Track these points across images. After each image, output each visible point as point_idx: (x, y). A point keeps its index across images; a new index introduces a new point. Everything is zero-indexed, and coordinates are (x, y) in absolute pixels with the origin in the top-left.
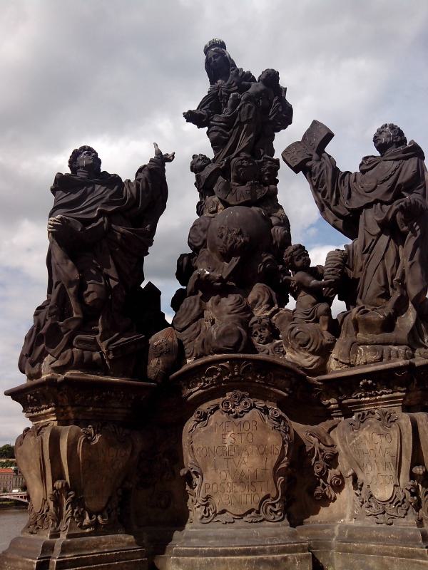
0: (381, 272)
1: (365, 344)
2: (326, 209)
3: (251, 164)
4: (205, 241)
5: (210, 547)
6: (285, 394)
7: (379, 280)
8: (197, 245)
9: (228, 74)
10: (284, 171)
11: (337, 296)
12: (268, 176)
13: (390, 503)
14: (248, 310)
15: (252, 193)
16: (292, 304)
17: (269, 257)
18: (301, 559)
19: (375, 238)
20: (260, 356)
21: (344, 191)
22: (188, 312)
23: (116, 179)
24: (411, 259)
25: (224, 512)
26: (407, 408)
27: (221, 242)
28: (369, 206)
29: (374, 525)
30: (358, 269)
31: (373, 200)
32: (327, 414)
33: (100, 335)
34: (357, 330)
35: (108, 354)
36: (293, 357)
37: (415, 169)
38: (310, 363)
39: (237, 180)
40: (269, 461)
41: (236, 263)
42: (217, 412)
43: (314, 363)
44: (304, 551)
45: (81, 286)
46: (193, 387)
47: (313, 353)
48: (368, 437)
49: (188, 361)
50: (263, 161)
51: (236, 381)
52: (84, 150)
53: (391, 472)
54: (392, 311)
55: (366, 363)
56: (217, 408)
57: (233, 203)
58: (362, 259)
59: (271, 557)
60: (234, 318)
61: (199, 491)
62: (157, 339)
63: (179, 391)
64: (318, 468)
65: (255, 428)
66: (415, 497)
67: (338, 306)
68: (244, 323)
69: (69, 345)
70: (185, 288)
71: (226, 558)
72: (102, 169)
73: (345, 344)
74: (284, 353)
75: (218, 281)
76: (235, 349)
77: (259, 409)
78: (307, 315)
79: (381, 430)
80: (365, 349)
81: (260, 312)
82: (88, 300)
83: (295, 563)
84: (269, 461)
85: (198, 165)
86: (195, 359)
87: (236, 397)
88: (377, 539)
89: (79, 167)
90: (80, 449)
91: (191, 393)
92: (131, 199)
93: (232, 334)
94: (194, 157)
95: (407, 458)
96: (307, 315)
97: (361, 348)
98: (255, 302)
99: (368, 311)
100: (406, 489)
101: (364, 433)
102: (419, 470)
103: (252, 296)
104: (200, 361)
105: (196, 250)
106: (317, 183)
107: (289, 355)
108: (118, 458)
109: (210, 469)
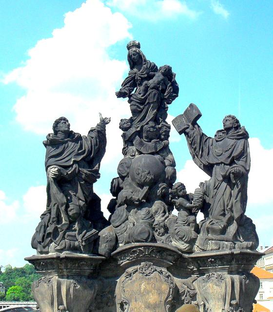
0: (222, 202)
2: (196, 157)
3: (155, 130)
4: (128, 173)
7: (220, 206)
8: (124, 175)
9: (141, 64)
10: (173, 132)
12: (164, 135)
14: (152, 217)
15: (156, 148)
16: (175, 212)
17: (164, 186)
19: (220, 182)
21: (206, 150)
22: (120, 217)
24: (236, 199)
26: (230, 273)
27: (138, 177)
28: (218, 164)
30: (211, 197)
31: (220, 162)
32: (193, 273)
33: (77, 232)
34: (208, 232)
35: (82, 242)
36: (176, 244)
37: (242, 147)
39: (147, 137)
41: (146, 190)
42: (137, 273)
45: (67, 207)
47: (186, 242)
49: (120, 245)
52: (61, 120)
53: (221, 303)
54: (226, 224)
55: (212, 250)
56: (137, 271)
58: (214, 192)
60: (145, 222)
62: (104, 233)
63: (117, 260)
67: (200, 216)
68: (151, 225)
69: (64, 238)
70: (115, 198)
73: (202, 239)
75: (137, 201)
76: (146, 241)
78: (184, 221)
80: (212, 242)
81: (158, 218)
82: (71, 213)
85: (125, 126)
86: (125, 244)
87: (147, 265)
89: (59, 131)
90: (71, 290)
91: (122, 263)
92: (89, 150)
93: (145, 232)
94: (121, 120)
95: (229, 296)
96: (184, 221)
98: (156, 212)
101: (209, 284)
102: (234, 302)
104: (128, 246)
105: (123, 178)
106: (192, 142)
107: (173, 243)
108: (88, 295)
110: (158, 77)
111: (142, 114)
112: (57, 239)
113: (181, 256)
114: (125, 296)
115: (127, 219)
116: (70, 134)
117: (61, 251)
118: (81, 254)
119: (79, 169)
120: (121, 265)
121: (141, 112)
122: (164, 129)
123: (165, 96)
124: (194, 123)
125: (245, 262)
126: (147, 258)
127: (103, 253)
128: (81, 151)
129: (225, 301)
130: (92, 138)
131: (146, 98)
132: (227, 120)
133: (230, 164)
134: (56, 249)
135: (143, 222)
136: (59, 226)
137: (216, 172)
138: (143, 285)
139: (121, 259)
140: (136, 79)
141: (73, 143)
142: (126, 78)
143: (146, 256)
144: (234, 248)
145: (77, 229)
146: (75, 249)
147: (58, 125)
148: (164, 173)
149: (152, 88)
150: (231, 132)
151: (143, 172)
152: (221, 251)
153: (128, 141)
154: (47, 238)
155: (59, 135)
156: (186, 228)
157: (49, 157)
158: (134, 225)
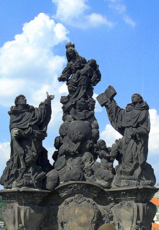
3: (85, 104)
4: (66, 134)
6: (96, 196)
7: (130, 156)
8: (63, 135)
9: (75, 59)
10: (97, 105)
12: (91, 107)
14: (83, 163)
15: (85, 116)
16: (99, 160)
20: (87, 182)
21: (120, 118)
22: (61, 164)
24: (140, 151)
26: (136, 202)
27: (73, 136)
28: (128, 127)
30: (123, 150)
33: (31, 174)
34: (121, 174)
35: (35, 181)
36: (99, 182)
38: (105, 184)
39: (79, 109)
41: (79, 145)
42: (72, 202)
43: (107, 184)
45: (25, 156)
46: (63, 192)
47: (106, 181)
49: (61, 183)
50: (89, 101)
53: (130, 222)
54: (133, 168)
55: (124, 186)
56: (72, 200)
58: (125, 146)
60: (78, 167)
61: (66, 229)
62: (50, 174)
63: (58, 193)
64: (106, 221)
67: (116, 163)
69: (22, 178)
70: (57, 150)
73: (117, 179)
74: (96, 180)
75: (72, 153)
76: (79, 180)
79: (128, 209)
80: (124, 181)
81: (87, 164)
82: (27, 161)
85: (64, 101)
87: (79, 196)
90: (27, 214)
91: (62, 195)
92: (39, 117)
93: (78, 174)
95: (135, 218)
97: (122, 180)
98: (86, 160)
99: (125, 168)
101: (122, 210)
102: (139, 222)
103: (84, 157)
104: (66, 183)
105: (62, 136)
106: (110, 112)
107: (97, 181)
108: (39, 217)
109: (70, 221)
110: (87, 67)
111: (76, 93)
112: (18, 179)
113: (102, 190)
114: (64, 218)
115: (66, 165)
116: (27, 107)
117: (20, 187)
118: (34, 189)
119: (33, 131)
120: (62, 196)
121: (75, 91)
122: (91, 103)
123: (92, 80)
124: (112, 99)
126: (80, 192)
127: (49, 188)
128: (34, 118)
129: (133, 221)
130: (42, 109)
131: (78, 82)
132: (134, 97)
133: (136, 127)
134: (17, 185)
135: (77, 167)
136: (19, 170)
137: (126, 132)
138: (76, 210)
139: (62, 193)
140: (72, 68)
141: (29, 113)
142: (65, 68)
143: (78, 190)
144: (139, 185)
145: (32, 172)
146: (30, 186)
147: (18, 100)
148: (91, 133)
149: (83, 75)
150: (137, 105)
151: (77, 132)
152: (130, 187)
153: (66, 111)
154: (11, 177)
155: (19, 107)
156: (106, 170)
157: (12, 122)
158: (70, 169)
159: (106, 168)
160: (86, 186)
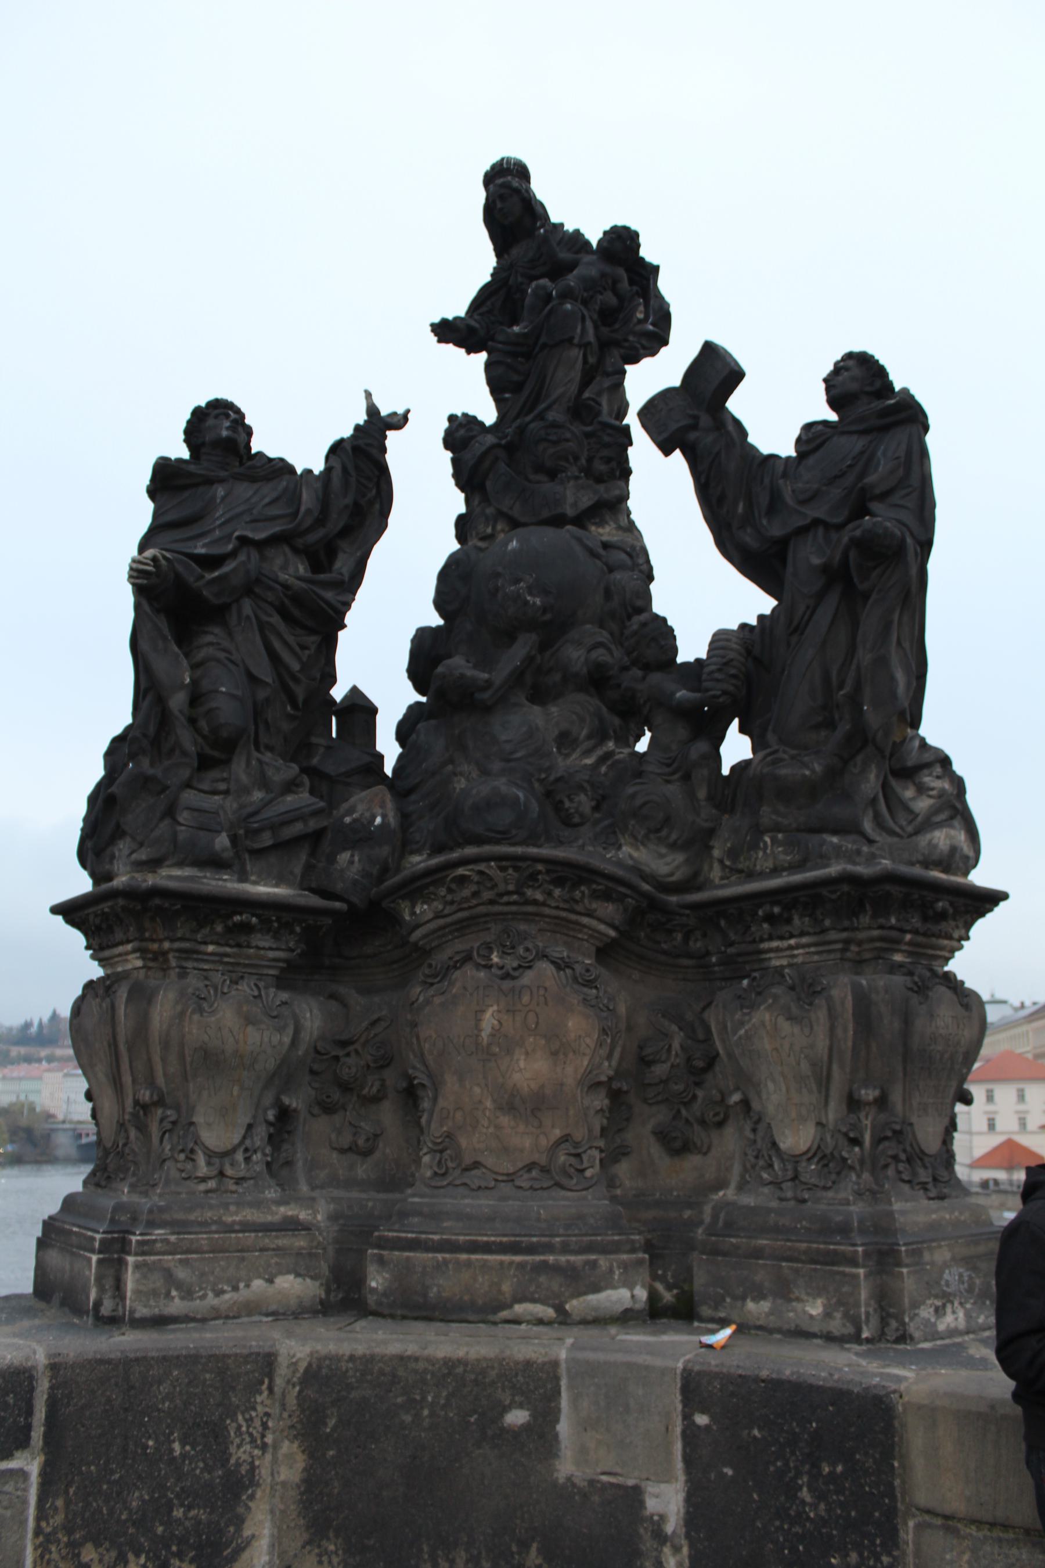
1: (777, 828)
5: (442, 1233)
6: (612, 933)
11: (736, 723)
13: (809, 1159)
18: (625, 1266)
23: (282, 467)
25: (477, 1165)
29: (774, 1204)
36: (635, 854)
40: (569, 1070)
43: (678, 867)
44: (633, 1251)
47: (673, 846)
48: (767, 1023)
51: (508, 903)
57: (523, 520)
59: (563, 1259)
65: (542, 999)
66: (857, 1149)
71: (473, 1257)
72: (256, 446)
77: (553, 962)
79: (795, 1010)
80: (774, 840)
83: (611, 1271)
84: (569, 1070)
88: (777, 1230)
89: (203, 444)
94: (452, 418)
96: (668, 765)
99: (781, 760)
100: (839, 1131)
101: (763, 1015)
113: (654, 905)
117: (154, 864)
125: (916, 921)
126: (514, 908)
129: (827, 1090)
159: (673, 773)
160: (548, 872)
